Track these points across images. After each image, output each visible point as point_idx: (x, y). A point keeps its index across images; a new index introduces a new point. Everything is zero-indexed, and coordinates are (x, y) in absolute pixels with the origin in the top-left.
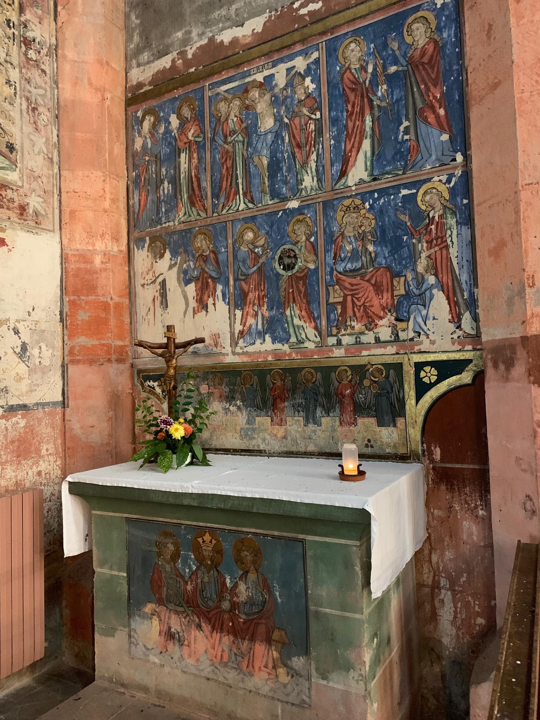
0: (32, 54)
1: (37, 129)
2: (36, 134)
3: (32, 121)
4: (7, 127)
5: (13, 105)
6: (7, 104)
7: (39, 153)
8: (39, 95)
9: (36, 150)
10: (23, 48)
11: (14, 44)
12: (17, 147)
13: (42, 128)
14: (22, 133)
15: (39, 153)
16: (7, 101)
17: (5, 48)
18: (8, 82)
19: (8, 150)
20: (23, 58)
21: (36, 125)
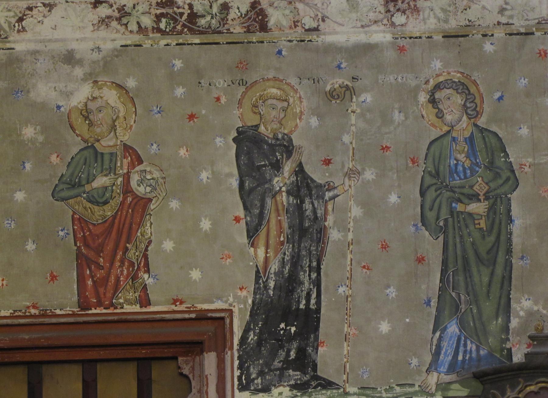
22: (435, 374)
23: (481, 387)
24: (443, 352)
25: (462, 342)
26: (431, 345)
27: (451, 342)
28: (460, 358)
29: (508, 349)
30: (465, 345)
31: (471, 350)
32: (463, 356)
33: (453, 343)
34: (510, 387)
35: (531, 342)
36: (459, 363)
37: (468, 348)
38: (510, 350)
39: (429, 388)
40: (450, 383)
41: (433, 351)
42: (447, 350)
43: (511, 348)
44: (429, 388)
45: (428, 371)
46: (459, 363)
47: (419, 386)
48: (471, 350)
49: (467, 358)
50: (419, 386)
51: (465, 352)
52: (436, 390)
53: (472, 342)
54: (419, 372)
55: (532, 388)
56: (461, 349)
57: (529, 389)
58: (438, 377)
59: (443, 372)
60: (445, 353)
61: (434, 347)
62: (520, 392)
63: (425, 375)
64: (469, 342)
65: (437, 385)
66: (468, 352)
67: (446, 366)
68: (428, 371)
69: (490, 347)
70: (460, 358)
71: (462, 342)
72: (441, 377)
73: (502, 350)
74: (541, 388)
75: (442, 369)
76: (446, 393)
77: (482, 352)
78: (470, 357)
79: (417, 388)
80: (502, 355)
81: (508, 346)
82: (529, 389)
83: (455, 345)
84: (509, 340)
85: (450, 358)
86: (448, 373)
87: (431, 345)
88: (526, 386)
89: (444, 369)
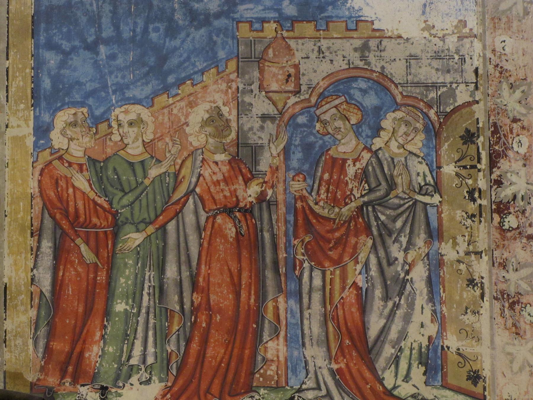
0: (511, 221)
1: (517, 334)
2: (516, 342)
3: (510, 323)
4: (469, 350)
5: (478, 312)
6: (469, 315)
7: (521, 369)
8: (522, 279)
9: (516, 367)
10: (497, 218)
11: (481, 221)
12: (486, 373)
13: (528, 327)
14: (493, 349)
15: (521, 369)
16: (469, 311)
17: (466, 234)
18: (471, 282)
19: (470, 382)
20: (496, 234)
21: (516, 328)
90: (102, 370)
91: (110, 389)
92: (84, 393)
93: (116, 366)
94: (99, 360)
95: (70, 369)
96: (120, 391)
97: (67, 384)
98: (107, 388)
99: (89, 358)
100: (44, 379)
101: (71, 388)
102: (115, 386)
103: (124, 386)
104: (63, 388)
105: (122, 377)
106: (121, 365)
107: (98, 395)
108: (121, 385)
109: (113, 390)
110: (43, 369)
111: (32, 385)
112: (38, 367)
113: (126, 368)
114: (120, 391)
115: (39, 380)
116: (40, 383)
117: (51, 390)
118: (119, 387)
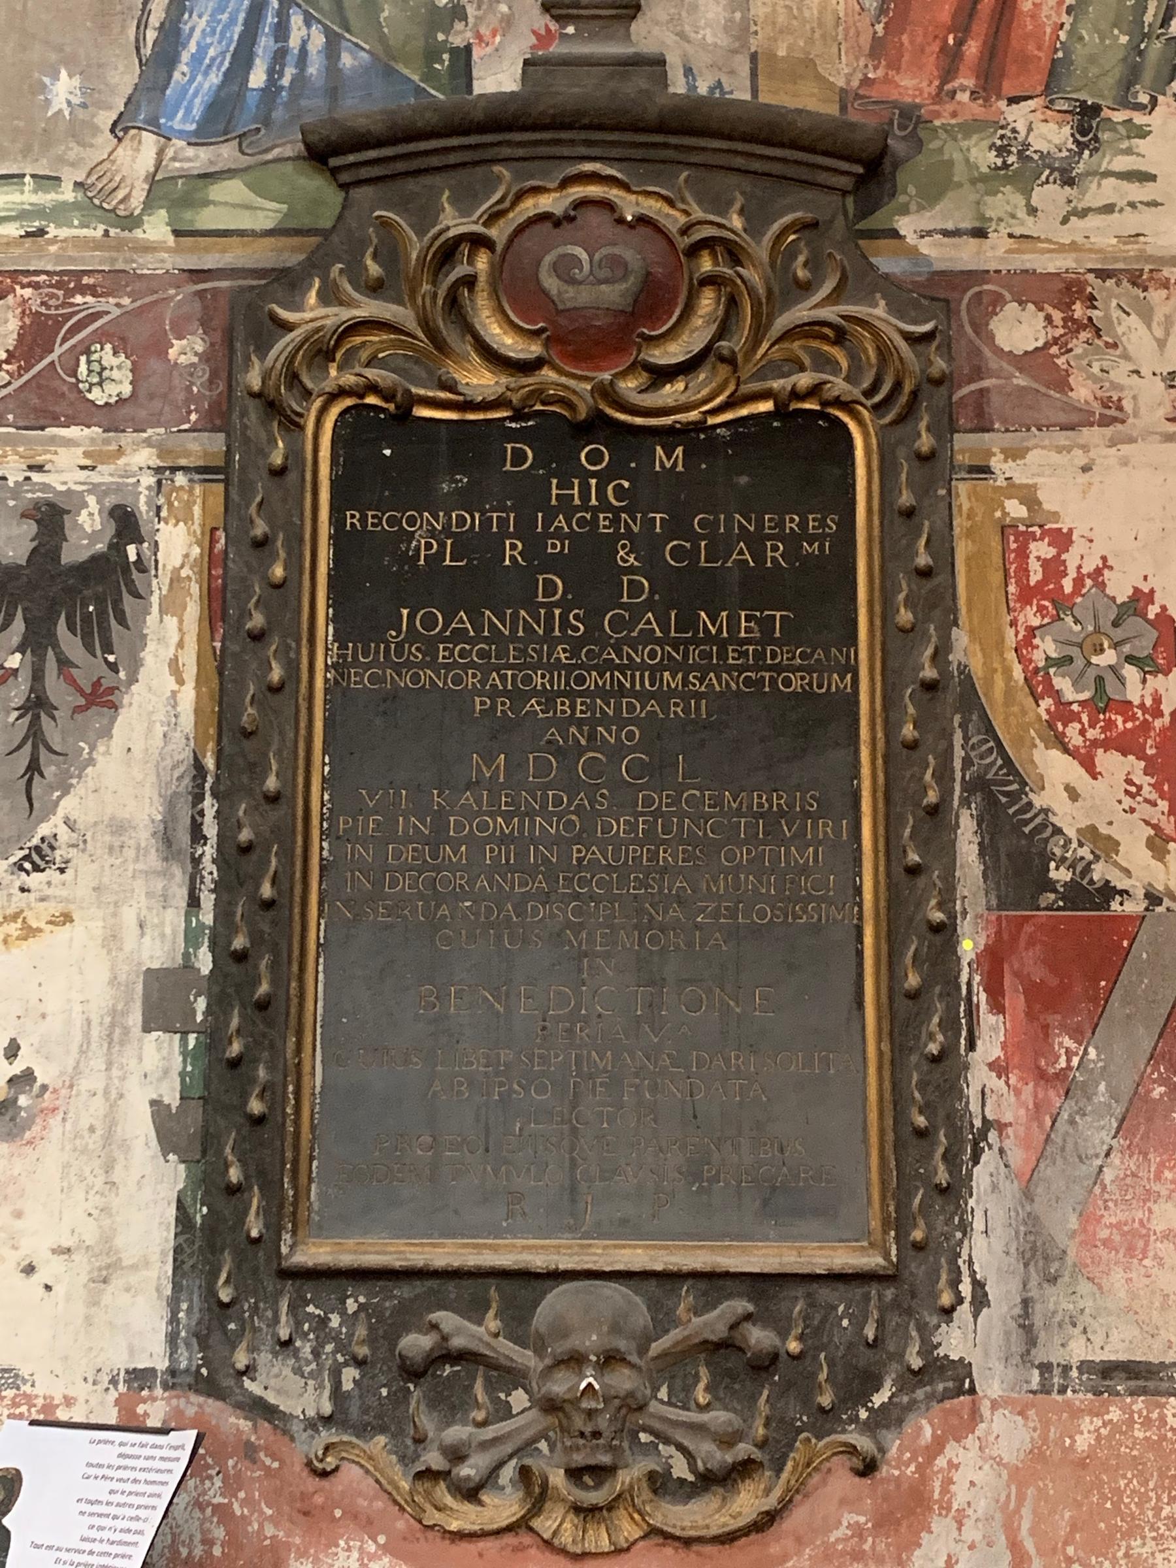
22: (149, 141)
23: (334, 197)
24: (185, 57)
25: (270, 19)
26: (142, 25)
27: (225, 17)
28: (257, 78)
29: (454, 51)
30: (282, 31)
31: (303, 51)
32: (271, 72)
33: (232, 21)
34: (453, 201)
35: (553, 26)
36: (252, 100)
37: (294, 42)
38: (463, 57)
39: (120, 194)
40: (208, 177)
41: (147, 51)
42: (202, 49)
43: (468, 49)
44: (120, 194)
45: (119, 128)
46: (252, 100)
47: (78, 185)
48: (303, 51)
49: (286, 81)
50: (78, 185)
51: (280, 56)
52: (149, 204)
53: (308, 20)
54: (79, 131)
55: (546, 203)
56: (265, 44)
57: (531, 206)
58: (160, 153)
59: (181, 134)
60: (197, 59)
61: (151, 35)
62: (494, 217)
63: (105, 139)
64: (296, 20)
65: (152, 180)
66: (291, 59)
67: (197, 112)
68: (119, 128)
69: (382, 38)
70: (257, 78)
71: (270, 19)
72: (170, 153)
73: (432, 54)
74: (582, 204)
75: (177, 124)
76: (188, 215)
77: (347, 60)
78: (300, 79)
79: (68, 194)
80: (430, 76)
81: (457, 41)
82: (531, 206)
83: (238, 29)
84: (464, 18)
85: (215, 78)
86: (199, 138)
87: (142, 25)
88: (519, 197)
89: (182, 121)
90: (1080, 53)
91: (1106, 113)
92: (1021, 127)
93: (1124, 39)
94: (1067, 20)
95: (972, 48)
96: (1139, 119)
97: (964, 97)
98: (1096, 109)
99: (1034, 16)
100: (886, 80)
101: (976, 109)
102: (1125, 102)
103: (1154, 102)
104: (949, 107)
105: (1148, 75)
106: (1141, 35)
107: (1067, 130)
108: (1144, 99)
109: (1119, 116)
110: (877, 49)
111: (845, 98)
112: (865, 41)
113: (1158, 45)
114: (1139, 119)
115: (866, 81)
116: (874, 93)
117: (909, 115)
118: (1139, 107)
